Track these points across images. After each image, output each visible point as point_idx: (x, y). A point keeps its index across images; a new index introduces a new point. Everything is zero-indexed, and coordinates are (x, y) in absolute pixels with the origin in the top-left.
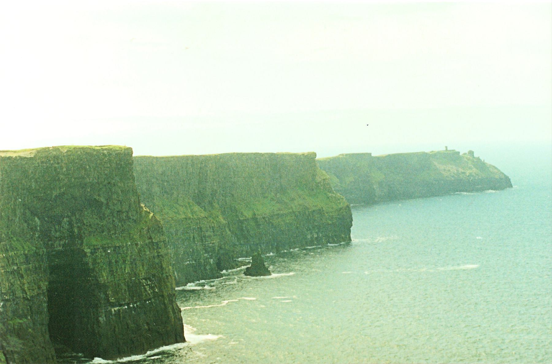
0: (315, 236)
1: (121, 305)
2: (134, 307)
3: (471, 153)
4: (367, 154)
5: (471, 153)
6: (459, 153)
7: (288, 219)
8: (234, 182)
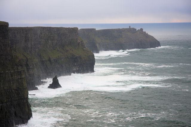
0: (78, 69)
3: (142, 30)
4: (93, 29)
5: (142, 30)
8: (40, 42)
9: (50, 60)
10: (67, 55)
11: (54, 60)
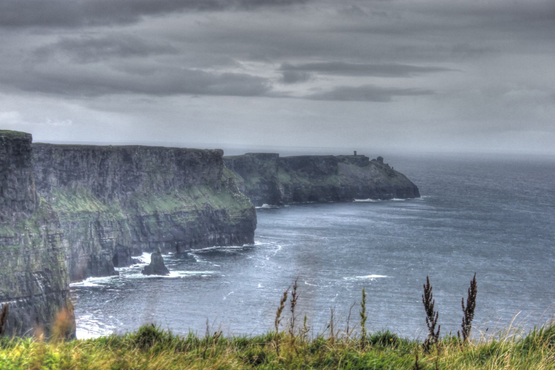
0: (218, 236)
1: (9, 299)
2: (23, 301)
3: (380, 159)
6: (367, 158)
7: (191, 218)
8: (137, 177)
9: (156, 215)
10: (195, 206)
11: (166, 215)
